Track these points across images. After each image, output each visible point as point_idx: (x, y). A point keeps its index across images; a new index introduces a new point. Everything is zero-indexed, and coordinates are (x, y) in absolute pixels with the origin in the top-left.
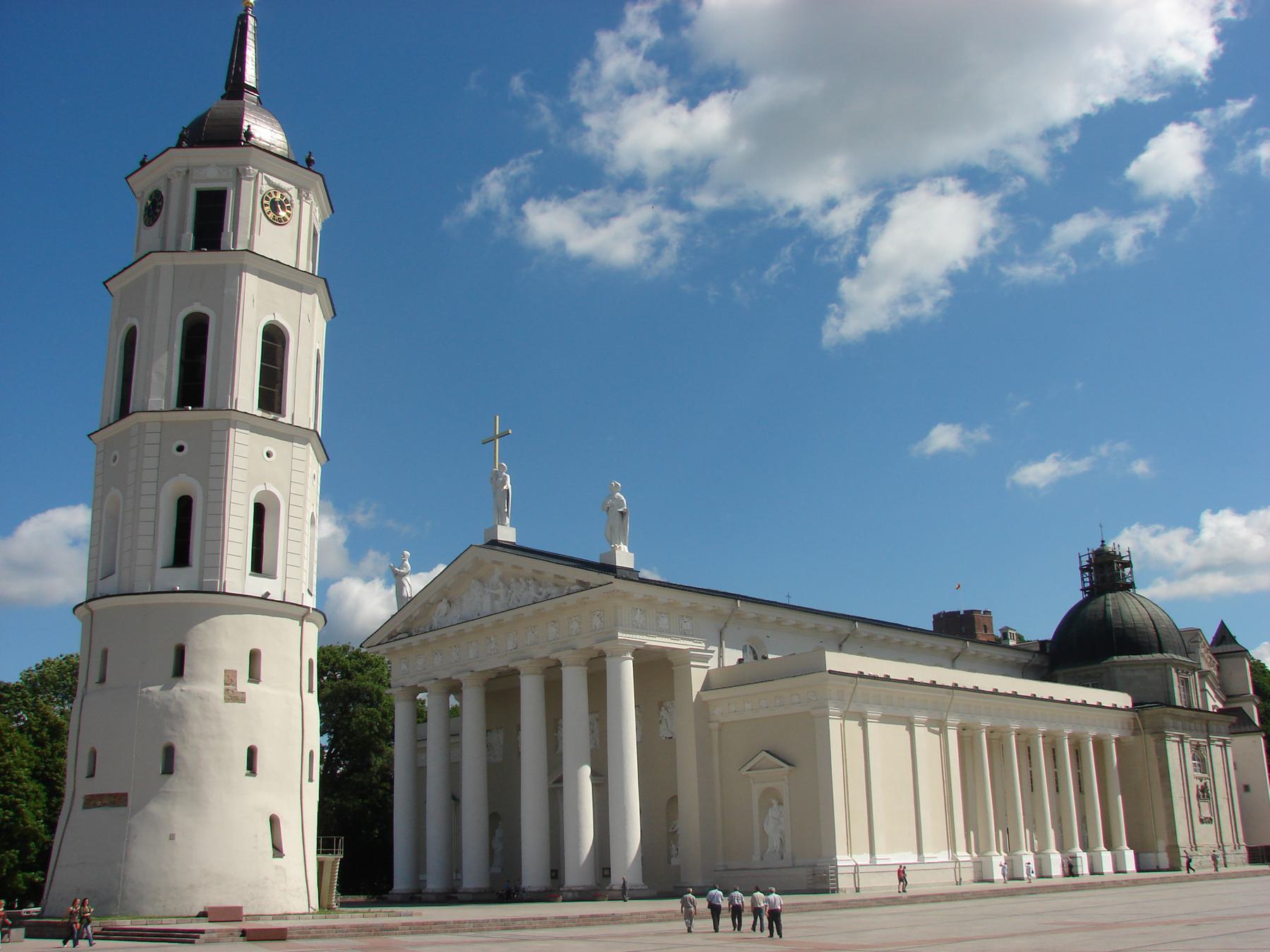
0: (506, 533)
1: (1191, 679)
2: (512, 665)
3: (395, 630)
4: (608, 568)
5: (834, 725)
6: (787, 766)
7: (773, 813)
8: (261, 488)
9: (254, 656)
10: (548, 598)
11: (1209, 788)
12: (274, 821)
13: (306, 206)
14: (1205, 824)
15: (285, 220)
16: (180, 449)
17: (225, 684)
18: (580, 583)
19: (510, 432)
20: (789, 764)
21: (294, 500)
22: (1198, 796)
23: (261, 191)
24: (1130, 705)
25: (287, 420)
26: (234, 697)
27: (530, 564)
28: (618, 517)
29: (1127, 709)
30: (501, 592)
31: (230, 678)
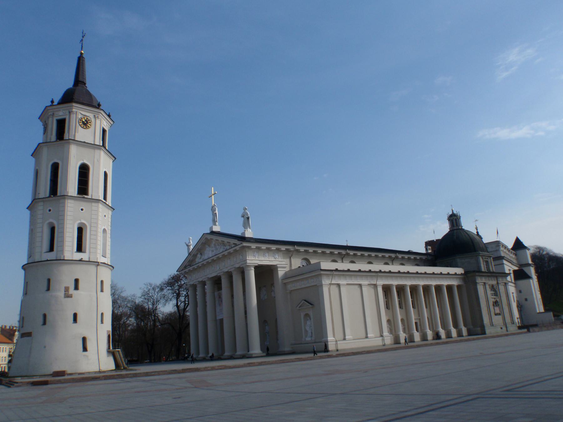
0: (216, 229)
1: (489, 260)
2: (219, 275)
3: (186, 265)
4: (242, 239)
5: (325, 290)
6: (310, 305)
7: (308, 323)
8: (79, 222)
9: (77, 281)
10: (226, 250)
11: (499, 301)
12: (84, 339)
13: (98, 122)
14: (497, 316)
15: (89, 127)
16: (50, 210)
17: (65, 291)
18: (234, 244)
19: (216, 192)
20: (311, 304)
21: (93, 225)
22: (493, 305)
23: (78, 118)
24: (463, 272)
25: (89, 197)
26: (68, 296)
27: (220, 239)
28: (246, 219)
29: (462, 274)
30: (214, 249)
31: (67, 289)
